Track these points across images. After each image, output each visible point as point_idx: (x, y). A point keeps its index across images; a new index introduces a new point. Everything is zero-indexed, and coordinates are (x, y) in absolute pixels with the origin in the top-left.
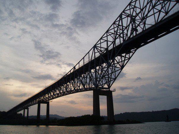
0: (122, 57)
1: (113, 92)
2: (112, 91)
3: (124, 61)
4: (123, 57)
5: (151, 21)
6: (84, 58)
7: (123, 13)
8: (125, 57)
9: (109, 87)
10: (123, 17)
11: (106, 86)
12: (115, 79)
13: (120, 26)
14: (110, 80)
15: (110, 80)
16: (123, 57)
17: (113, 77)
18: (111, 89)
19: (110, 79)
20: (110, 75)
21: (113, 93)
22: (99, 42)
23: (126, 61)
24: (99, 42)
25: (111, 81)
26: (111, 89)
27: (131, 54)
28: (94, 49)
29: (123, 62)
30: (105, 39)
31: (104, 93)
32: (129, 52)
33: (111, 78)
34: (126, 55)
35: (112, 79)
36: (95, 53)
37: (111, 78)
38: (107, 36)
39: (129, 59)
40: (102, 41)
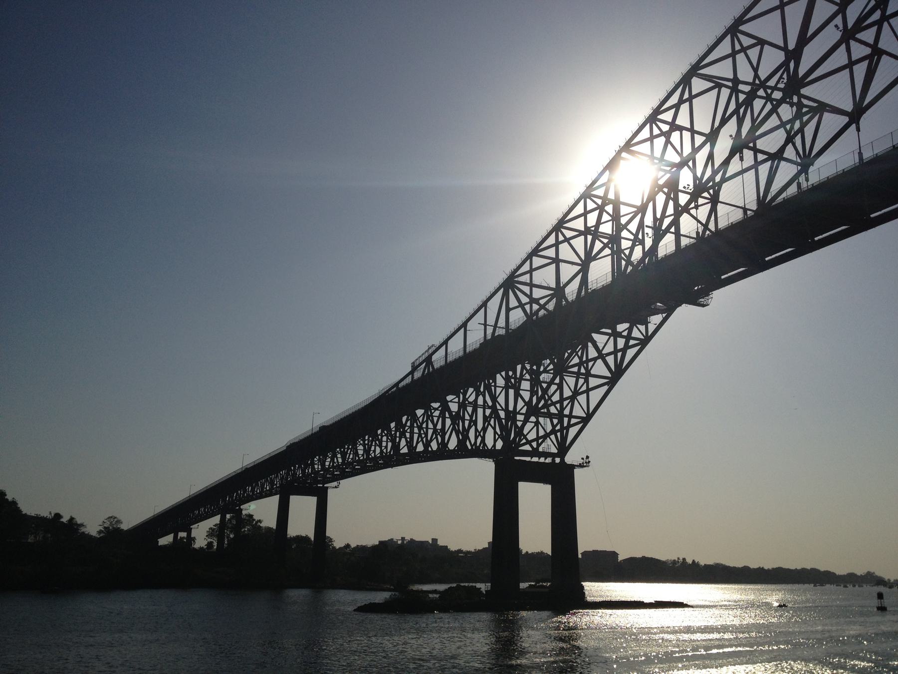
0: (616, 335)
1: (577, 472)
3: (624, 351)
8: (629, 338)
9: (563, 448)
12: (585, 421)
14: (565, 424)
15: (565, 424)
18: (570, 458)
19: (566, 420)
22: (526, 267)
23: (630, 353)
24: (526, 267)
25: (570, 426)
26: (570, 458)
29: (619, 354)
30: (551, 253)
33: (570, 416)
34: (630, 330)
35: (573, 421)
36: (508, 310)
38: (557, 244)
39: (644, 342)
40: (537, 261)
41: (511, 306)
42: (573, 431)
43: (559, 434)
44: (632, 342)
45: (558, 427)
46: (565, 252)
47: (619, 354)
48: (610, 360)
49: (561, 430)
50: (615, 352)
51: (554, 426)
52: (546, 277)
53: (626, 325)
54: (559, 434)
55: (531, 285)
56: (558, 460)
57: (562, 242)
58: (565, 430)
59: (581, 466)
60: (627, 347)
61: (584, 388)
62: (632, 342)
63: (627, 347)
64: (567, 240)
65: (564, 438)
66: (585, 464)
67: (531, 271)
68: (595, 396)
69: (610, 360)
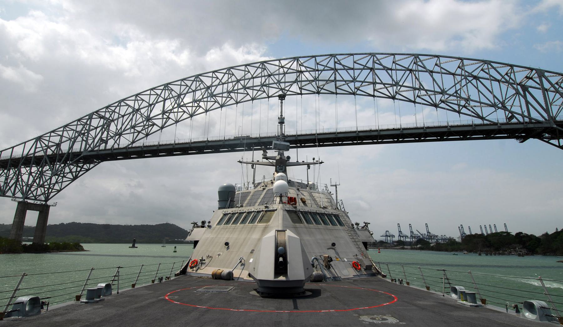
0: (78, 166)
1: (51, 208)
2: (50, 206)
3: (79, 172)
4: (80, 167)
5: (124, 142)
6: (13, 148)
7: (95, 113)
8: (82, 167)
9: (47, 199)
10: (94, 116)
11: (42, 198)
12: (59, 191)
13: (87, 124)
14: (50, 192)
15: (50, 192)
16: (80, 167)
17: (57, 187)
19: (50, 190)
20: (51, 186)
21: (51, 209)
22: (49, 135)
23: (81, 173)
25: (51, 192)
27: (92, 165)
28: (36, 142)
30: (61, 133)
31: (33, 207)
32: (90, 163)
34: (83, 166)
36: (36, 148)
37: (53, 189)
38: (63, 131)
39: (87, 170)
40: (52, 134)
41: (37, 147)
42: (52, 194)
43: (46, 195)
44: (83, 169)
45: (46, 192)
46: (65, 134)
47: (77, 173)
48: (74, 174)
49: (47, 194)
50: (76, 172)
51: (45, 191)
52: (56, 140)
53: (82, 165)
54: (46, 195)
55: (49, 141)
56: (44, 203)
57: (65, 131)
58: (49, 194)
59: (53, 206)
60: (81, 171)
61: (61, 181)
62: (83, 169)
63: (81, 171)
64: (67, 131)
65: (48, 196)
66: (55, 205)
67: (50, 136)
68: (64, 184)
69: (74, 174)
